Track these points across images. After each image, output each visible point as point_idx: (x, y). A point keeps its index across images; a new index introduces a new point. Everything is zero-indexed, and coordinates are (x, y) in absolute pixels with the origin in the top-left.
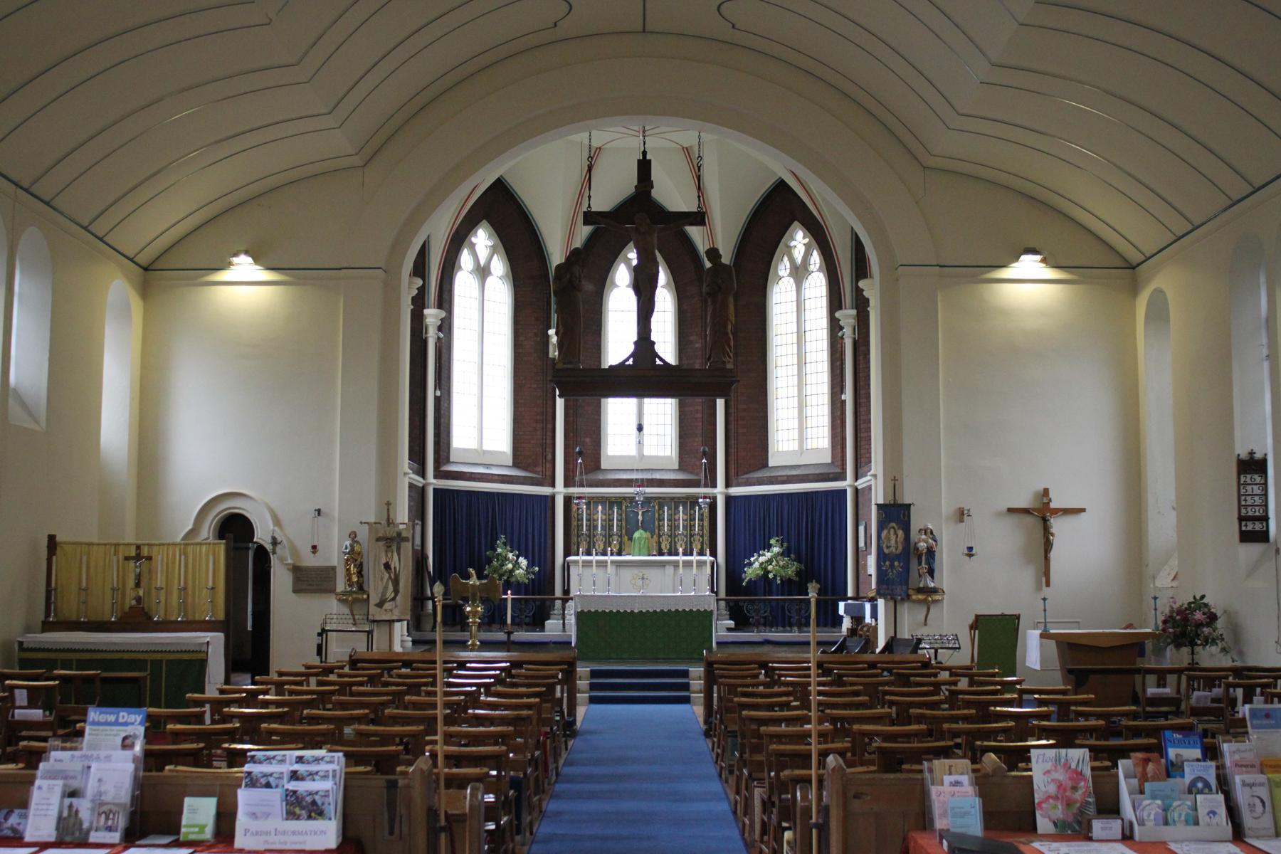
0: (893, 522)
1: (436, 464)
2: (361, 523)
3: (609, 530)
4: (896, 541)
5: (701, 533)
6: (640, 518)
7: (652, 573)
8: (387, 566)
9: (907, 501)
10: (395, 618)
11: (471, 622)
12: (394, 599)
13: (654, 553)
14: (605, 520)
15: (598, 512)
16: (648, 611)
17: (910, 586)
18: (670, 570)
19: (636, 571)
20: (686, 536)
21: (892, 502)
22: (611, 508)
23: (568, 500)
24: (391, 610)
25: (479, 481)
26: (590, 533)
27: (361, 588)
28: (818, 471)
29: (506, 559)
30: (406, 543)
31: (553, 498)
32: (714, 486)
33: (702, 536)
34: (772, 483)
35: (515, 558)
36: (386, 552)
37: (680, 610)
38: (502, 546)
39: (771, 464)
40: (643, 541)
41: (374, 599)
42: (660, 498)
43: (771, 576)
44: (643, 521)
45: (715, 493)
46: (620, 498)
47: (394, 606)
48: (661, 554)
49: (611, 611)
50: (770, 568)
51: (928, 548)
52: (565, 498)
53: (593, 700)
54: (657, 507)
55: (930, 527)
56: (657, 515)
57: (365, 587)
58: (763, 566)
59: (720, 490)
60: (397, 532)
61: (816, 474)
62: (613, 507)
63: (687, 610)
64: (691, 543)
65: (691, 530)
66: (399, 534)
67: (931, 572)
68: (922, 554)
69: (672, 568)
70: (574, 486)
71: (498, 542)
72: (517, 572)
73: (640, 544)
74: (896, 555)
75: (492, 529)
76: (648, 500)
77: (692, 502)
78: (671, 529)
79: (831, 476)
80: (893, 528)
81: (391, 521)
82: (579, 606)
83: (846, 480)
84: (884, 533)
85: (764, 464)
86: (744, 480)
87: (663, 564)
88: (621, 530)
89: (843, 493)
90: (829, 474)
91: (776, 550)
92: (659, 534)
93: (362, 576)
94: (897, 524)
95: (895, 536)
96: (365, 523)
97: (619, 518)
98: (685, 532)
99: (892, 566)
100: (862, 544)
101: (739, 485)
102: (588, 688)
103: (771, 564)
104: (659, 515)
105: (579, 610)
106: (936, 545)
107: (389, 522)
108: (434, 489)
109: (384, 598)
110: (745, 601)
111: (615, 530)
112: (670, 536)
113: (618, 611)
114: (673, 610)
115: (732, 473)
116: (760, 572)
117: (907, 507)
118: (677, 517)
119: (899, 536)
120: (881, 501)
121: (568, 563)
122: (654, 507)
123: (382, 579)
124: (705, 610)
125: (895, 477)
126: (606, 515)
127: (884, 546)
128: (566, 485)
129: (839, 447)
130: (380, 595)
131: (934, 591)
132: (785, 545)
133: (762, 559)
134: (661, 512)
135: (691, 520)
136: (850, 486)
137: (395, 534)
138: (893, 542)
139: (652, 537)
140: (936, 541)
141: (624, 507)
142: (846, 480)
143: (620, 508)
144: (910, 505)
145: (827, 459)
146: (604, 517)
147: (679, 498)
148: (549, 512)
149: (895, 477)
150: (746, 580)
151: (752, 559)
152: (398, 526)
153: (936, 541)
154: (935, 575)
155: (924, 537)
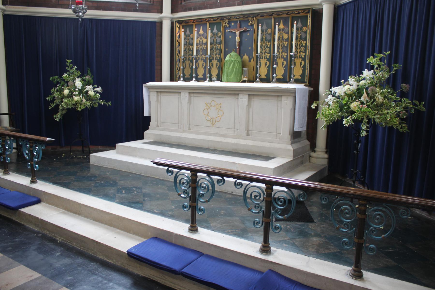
5: (303, 55)
6: (238, 39)
13: (244, 79)
19: (208, 99)
31: (161, 23)
33: (304, 59)
42: (258, 14)
44: (240, 43)
46: (218, 18)
50: (354, 105)
69: (246, 97)
87: (235, 92)
122: (252, 25)
128: (173, 11)
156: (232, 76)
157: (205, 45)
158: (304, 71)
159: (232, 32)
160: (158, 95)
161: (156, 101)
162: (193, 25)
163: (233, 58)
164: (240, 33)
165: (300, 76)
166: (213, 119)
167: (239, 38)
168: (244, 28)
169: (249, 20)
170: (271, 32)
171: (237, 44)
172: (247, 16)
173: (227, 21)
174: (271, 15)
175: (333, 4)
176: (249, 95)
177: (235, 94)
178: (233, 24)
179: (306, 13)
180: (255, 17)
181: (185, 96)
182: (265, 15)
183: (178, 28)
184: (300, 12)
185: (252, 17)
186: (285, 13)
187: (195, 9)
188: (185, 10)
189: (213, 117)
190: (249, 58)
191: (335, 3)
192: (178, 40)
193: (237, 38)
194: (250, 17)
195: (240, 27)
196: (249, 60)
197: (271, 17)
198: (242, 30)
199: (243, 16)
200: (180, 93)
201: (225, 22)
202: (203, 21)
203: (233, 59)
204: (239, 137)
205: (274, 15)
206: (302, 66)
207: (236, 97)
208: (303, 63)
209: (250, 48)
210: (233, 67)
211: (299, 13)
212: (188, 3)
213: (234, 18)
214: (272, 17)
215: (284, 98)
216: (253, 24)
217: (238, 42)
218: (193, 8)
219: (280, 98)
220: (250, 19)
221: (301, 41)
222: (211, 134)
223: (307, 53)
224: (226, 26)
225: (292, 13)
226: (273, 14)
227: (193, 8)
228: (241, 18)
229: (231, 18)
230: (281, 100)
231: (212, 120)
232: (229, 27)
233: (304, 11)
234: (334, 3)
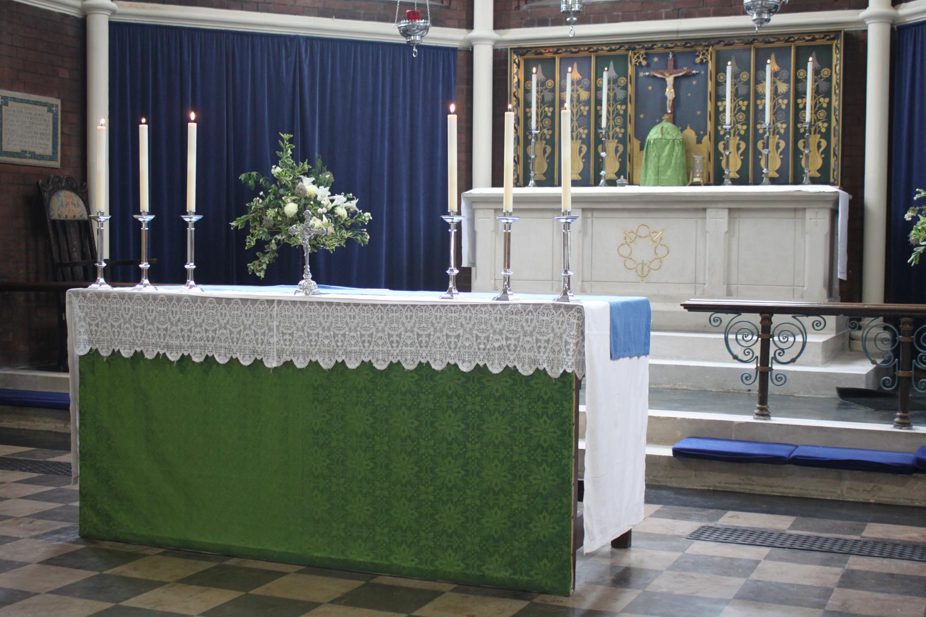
5: (823, 127)
6: (670, 93)
13: (696, 180)
16: (314, 365)
18: (718, 220)
19: (631, 223)
20: (784, 137)
25: (258, 10)
31: (469, 53)
33: (826, 136)
37: (437, 366)
40: (668, 148)
42: (719, 40)
44: (676, 101)
45: (862, 22)
46: (621, 45)
52: (496, 52)
54: (711, 66)
56: (710, 86)
63: (465, 368)
69: (725, 213)
73: (659, 158)
87: (699, 206)
92: (717, 132)
98: (782, 127)
108: (113, 26)
112: (744, 138)
114: (409, 366)
122: (704, 64)
126: (588, 89)
128: (499, 24)
139: (699, 141)
141: (631, 70)
146: (584, 95)
156: (669, 173)
157: (584, 106)
158: (826, 161)
159: (655, 77)
161: (493, 231)
162: (554, 59)
163: (668, 133)
164: (675, 78)
165: (819, 171)
166: (643, 264)
167: (673, 90)
168: (684, 70)
169: (697, 52)
170: (749, 79)
171: (669, 103)
172: (693, 44)
173: (643, 52)
174: (751, 43)
175: (888, 23)
176: (730, 210)
177: (696, 210)
178: (656, 59)
179: (828, 40)
180: (713, 46)
182: (737, 41)
183: (515, 66)
184: (817, 37)
185: (705, 46)
186: (782, 39)
188: (530, 24)
189: (643, 261)
190: (697, 134)
191: (894, 21)
192: (516, 94)
193: (667, 90)
194: (700, 45)
195: (675, 67)
196: (697, 138)
197: (749, 46)
198: (680, 74)
199: (683, 44)
201: (637, 55)
202: (582, 51)
203: (669, 137)
205: (757, 44)
206: (821, 150)
207: (700, 215)
208: (824, 144)
209: (699, 113)
210: (670, 155)
211: (814, 39)
212: (537, 7)
213: (660, 47)
214: (752, 46)
215: (809, 214)
216: (707, 62)
217: (671, 99)
218: (550, 19)
219: (799, 215)
220: (700, 48)
221: (817, 98)
223: (834, 123)
224: (640, 63)
225: (799, 39)
226: (754, 40)
227: (550, 19)
228: (678, 46)
229: (655, 46)
230: (804, 218)
231: (639, 267)
232: (648, 65)
233: (826, 36)
234: (891, 22)
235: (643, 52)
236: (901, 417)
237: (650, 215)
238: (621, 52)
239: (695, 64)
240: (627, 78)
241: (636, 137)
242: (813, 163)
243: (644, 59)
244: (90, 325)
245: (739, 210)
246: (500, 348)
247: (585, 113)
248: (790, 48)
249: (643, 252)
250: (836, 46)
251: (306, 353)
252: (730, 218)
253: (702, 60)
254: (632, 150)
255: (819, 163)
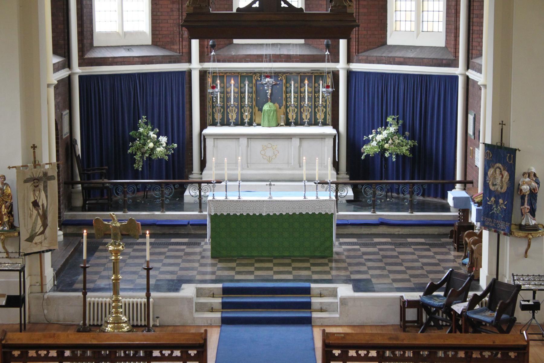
0: (500, 162)
1: (81, 53)
2: (9, 168)
3: (241, 102)
4: (501, 181)
7: (280, 144)
8: (35, 204)
9: (513, 146)
10: (44, 249)
11: (113, 260)
12: (43, 233)
13: (282, 124)
14: (237, 93)
15: (231, 85)
17: (513, 222)
19: (265, 143)
21: (499, 144)
22: (242, 82)
23: (203, 74)
24: (41, 243)
25: (121, 65)
26: (224, 105)
27: (12, 227)
28: (433, 56)
29: (148, 137)
30: (52, 181)
31: (189, 73)
32: (337, 61)
33: (325, 107)
34: (390, 63)
35: (156, 136)
36: (34, 190)
37: (304, 213)
38: (144, 125)
39: (391, 40)
40: (272, 113)
41: (25, 235)
42: (287, 73)
43: (387, 155)
44: (271, 94)
46: (251, 73)
47: (43, 238)
48: (288, 124)
49: (242, 215)
50: (386, 146)
51: (530, 189)
52: (200, 72)
53: (225, 321)
54: (284, 81)
55: (533, 170)
56: (284, 88)
57: (16, 224)
58: (380, 144)
59: (341, 66)
60: (43, 173)
61: (430, 58)
62: (245, 81)
63: (310, 213)
64: (315, 113)
65: (315, 102)
66: (45, 174)
67: (533, 212)
68: (526, 195)
69: (298, 140)
70: (209, 61)
71: (140, 121)
72: (158, 149)
73: (269, 116)
74: (501, 193)
75: (134, 102)
76: (276, 74)
77: (317, 76)
78: (298, 100)
79: (444, 62)
80: (500, 169)
81: (37, 163)
82: (213, 211)
83: (458, 67)
84: (491, 172)
85: (384, 43)
86: (364, 58)
87: (289, 137)
88: (252, 102)
89: (456, 78)
90: (443, 60)
91: (392, 129)
92: (286, 105)
93: (12, 216)
94: (503, 165)
95: (501, 176)
96: (13, 167)
97: (250, 90)
99: (497, 202)
100: (470, 131)
101: (359, 61)
102: (220, 307)
103: (387, 143)
104: (286, 88)
105: (213, 214)
106: (539, 187)
107: (36, 164)
109: (34, 233)
110: (362, 184)
111: (246, 103)
112: (296, 107)
113: (248, 215)
114: (297, 213)
115: (353, 50)
116: (377, 150)
117: (513, 152)
118: (302, 90)
119: (504, 177)
120: (489, 141)
121: (204, 136)
123: (31, 216)
124: (326, 213)
125: (502, 121)
126: (238, 88)
127: (490, 183)
129: (453, 35)
130: (30, 231)
131: (535, 228)
132: (401, 122)
133: (379, 137)
134: (288, 85)
135: (315, 93)
136: (461, 74)
137: (41, 175)
138: (498, 181)
139: (280, 108)
140: (538, 183)
141: (254, 81)
142: (458, 67)
143: (250, 82)
144: (516, 150)
145: (441, 42)
147: (304, 73)
148: (186, 86)
149: (502, 121)
150: (365, 154)
151: (370, 136)
152: (44, 167)
153: (538, 183)
154: (536, 213)
155: (527, 180)
158: (325, 116)
160: (214, 141)
162: (224, 76)
163: (272, 107)
170: (298, 86)
173: (259, 75)
174: (299, 74)
176: (300, 138)
181: (244, 141)
187: (224, 61)
200: (239, 138)
203: (272, 109)
204: (294, 169)
206: (324, 112)
207: (290, 140)
208: (324, 110)
210: (273, 115)
211: (321, 73)
215: (327, 140)
219: (323, 140)
220: (280, 75)
222: (269, 169)
223: (328, 103)
227: (221, 60)
235: (259, 75)
236: (373, 210)
237: (272, 140)
238: (251, 74)
239: (278, 80)
240: (252, 84)
241: (257, 106)
242: (320, 116)
243: (259, 77)
244: (214, 208)
245: (303, 138)
246: (318, 209)
247: (236, 97)
248: (312, 76)
249: (269, 153)
250: (329, 76)
251: (272, 212)
252: (300, 141)
253: (281, 79)
254: (255, 111)
255: (323, 117)
